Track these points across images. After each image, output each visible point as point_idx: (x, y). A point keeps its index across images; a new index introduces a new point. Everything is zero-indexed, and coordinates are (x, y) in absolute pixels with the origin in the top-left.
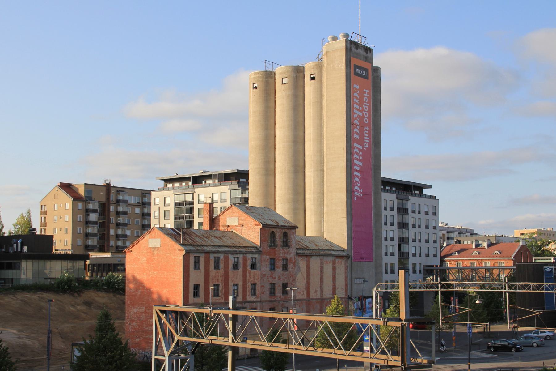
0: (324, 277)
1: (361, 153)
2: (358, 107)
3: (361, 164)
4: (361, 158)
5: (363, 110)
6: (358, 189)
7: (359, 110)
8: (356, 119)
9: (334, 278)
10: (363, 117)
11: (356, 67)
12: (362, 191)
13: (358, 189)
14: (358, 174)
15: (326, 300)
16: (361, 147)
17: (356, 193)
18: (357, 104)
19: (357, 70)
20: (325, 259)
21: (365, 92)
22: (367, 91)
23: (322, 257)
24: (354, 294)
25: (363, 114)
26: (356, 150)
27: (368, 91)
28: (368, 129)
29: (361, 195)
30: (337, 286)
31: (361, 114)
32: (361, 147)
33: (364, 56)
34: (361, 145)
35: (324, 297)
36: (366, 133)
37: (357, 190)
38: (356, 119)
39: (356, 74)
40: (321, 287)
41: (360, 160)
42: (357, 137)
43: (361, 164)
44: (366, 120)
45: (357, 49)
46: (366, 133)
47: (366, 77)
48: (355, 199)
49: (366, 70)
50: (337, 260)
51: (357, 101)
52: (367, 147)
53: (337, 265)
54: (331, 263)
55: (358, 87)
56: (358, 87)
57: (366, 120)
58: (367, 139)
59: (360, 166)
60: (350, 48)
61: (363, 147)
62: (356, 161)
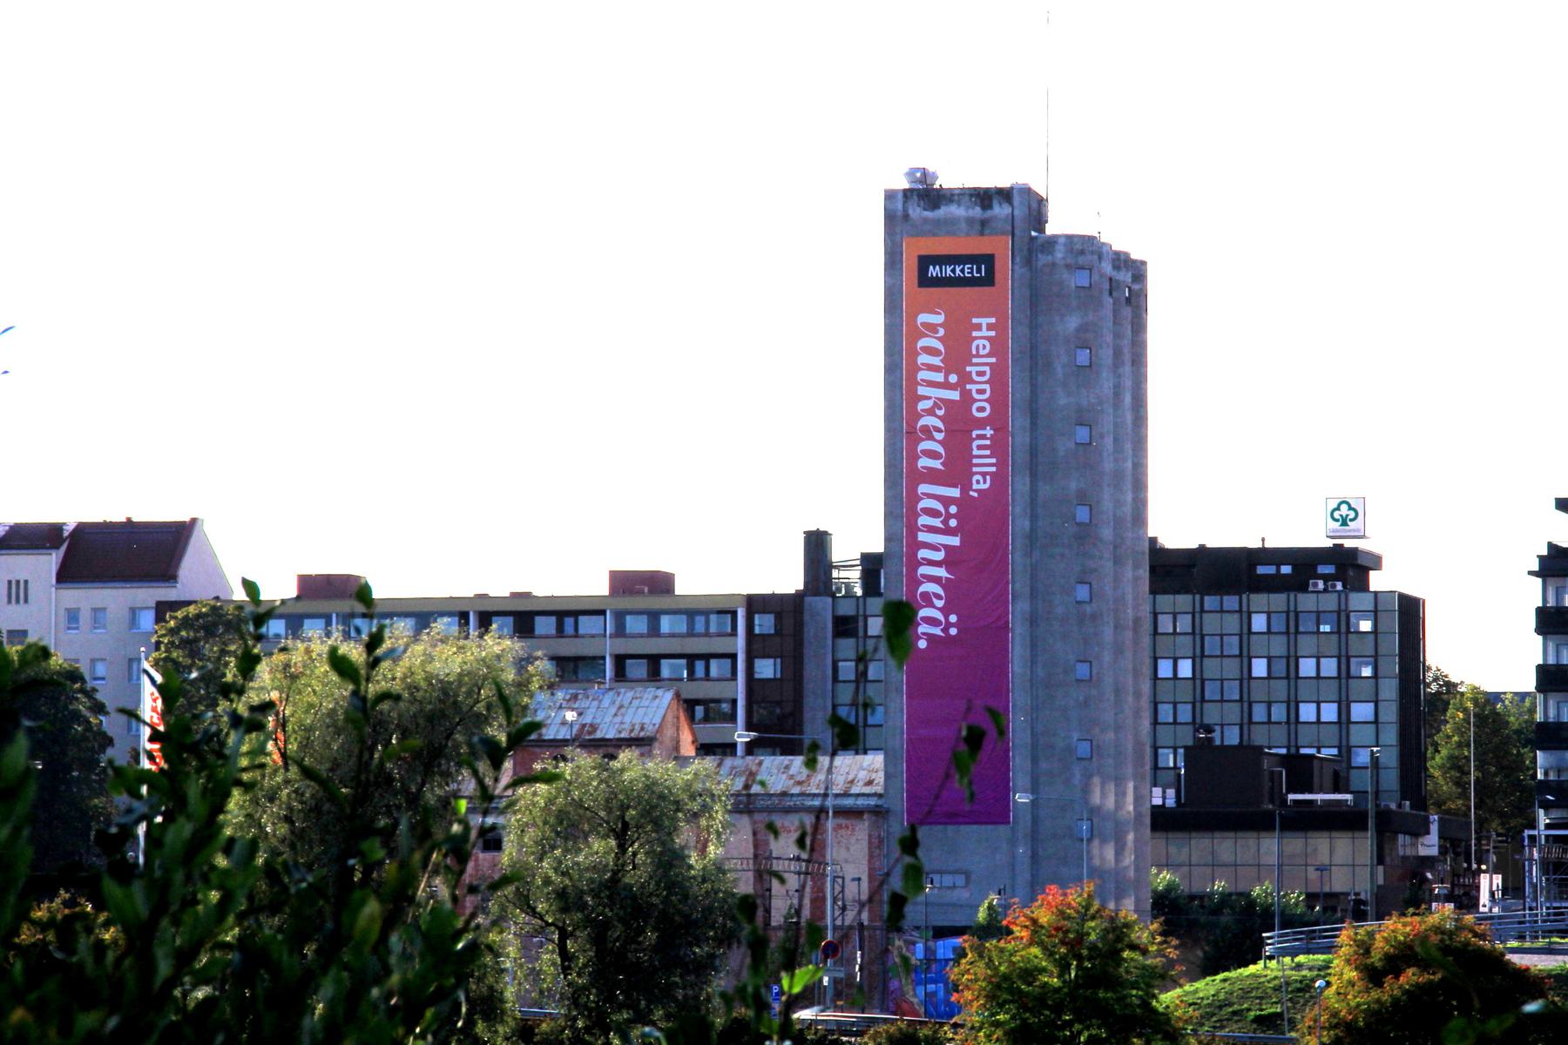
1: (953, 509)
2: (939, 377)
3: (955, 541)
4: (953, 523)
5: (965, 378)
6: (939, 615)
7: (946, 385)
8: (930, 412)
10: (967, 399)
11: (925, 262)
12: (953, 618)
13: (939, 615)
14: (941, 572)
16: (955, 492)
18: (931, 368)
19: (933, 271)
21: (979, 327)
22: (984, 321)
25: (966, 395)
26: (922, 505)
27: (993, 320)
28: (989, 432)
31: (955, 395)
32: (955, 492)
33: (970, 221)
34: (955, 486)
36: (980, 447)
37: (932, 621)
38: (930, 412)
39: (925, 281)
41: (947, 531)
42: (936, 464)
43: (955, 541)
44: (981, 409)
46: (980, 447)
47: (989, 280)
49: (988, 260)
51: (936, 361)
55: (938, 319)
56: (938, 319)
57: (981, 409)
58: (983, 464)
59: (946, 547)
60: (905, 210)
61: (966, 487)
62: (922, 537)
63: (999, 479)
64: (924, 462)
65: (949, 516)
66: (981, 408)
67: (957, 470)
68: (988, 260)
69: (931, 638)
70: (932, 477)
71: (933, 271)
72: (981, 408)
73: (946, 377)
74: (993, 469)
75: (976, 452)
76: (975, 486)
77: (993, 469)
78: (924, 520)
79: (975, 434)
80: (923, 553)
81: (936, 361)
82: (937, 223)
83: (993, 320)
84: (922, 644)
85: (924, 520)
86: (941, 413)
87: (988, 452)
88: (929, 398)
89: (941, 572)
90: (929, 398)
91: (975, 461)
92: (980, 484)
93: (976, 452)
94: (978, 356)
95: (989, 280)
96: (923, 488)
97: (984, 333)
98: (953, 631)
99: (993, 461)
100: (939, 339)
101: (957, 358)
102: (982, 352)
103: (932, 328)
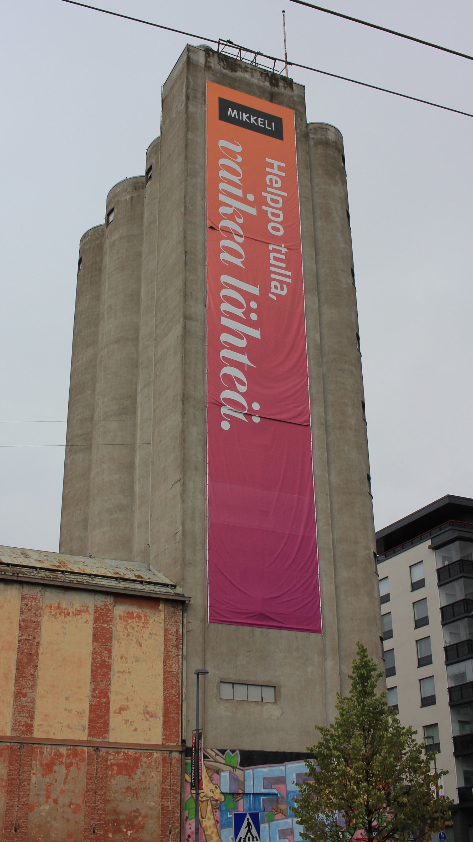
0: (44, 660)
2: (239, 193)
7: (244, 200)
8: (231, 217)
9: (101, 670)
12: (256, 406)
15: (47, 750)
17: (223, 410)
19: (232, 113)
20: (51, 598)
21: (272, 166)
23: (27, 591)
24: (213, 739)
26: (225, 292)
27: (283, 165)
29: (256, 420)
30: (115, 701)
31: (253, 211)
35: (37, 734)
40: (19, 695)
41: (248, 322)
45: (234, 70)
48: (225, 425)
50: (120, 610)
51: (236, 179)
52: (279, 292)
53: (118, 628)
54: (90, 617)
55: (238, 149)
56: (238, 149)
59: (249, 337)
61: (266, 289)
62: (225, 321)
63: (294, 289)
64: (224, 256)
65: (249, 311)
66: (276, 227)
67: (255, 271)
68: (279, 121)
69: (233, 420)
70: (232, 270)
71: (232, 113)
72: (276, 227)
73: (245, 194)
74: (290, 281)
75: (272, 262)
76: (273, 290)
77: (290, 281)
78: (225, 307)
79: (271, 247)
80: (224, 337)
81: (236, 179)
82: (235, 79)
83: (283, 165)
84: (225, 425)
85: (225, 307)
86: (241, 221)
87: (284, 265)
88: (230, 206)
89: (244, 359)
90: (230, 206)
91: (272, 269)
92: (278, 290)
93: (272, 262)
94: (271, 186)
95: (278, 134)
96: (224, 278)
97: (276, 171)
98: (256, 420)
99: (289, 273)
100: (237, 163)
101: (253, 182)
102: (274, 185)
103: (232, 155)
